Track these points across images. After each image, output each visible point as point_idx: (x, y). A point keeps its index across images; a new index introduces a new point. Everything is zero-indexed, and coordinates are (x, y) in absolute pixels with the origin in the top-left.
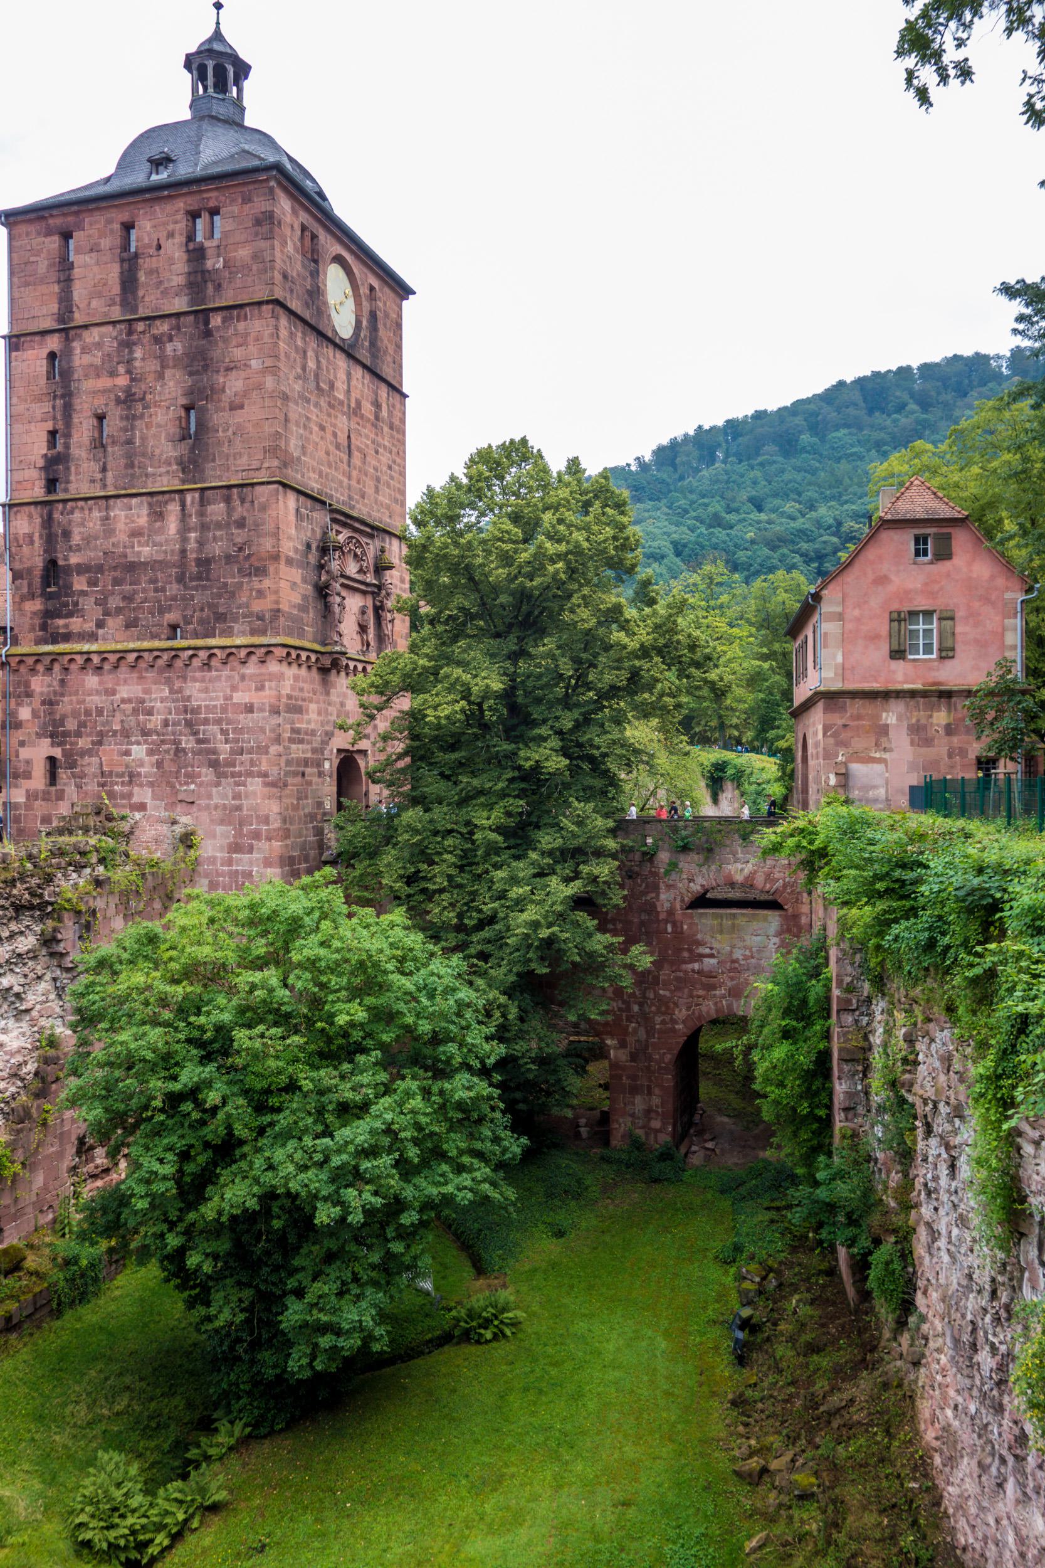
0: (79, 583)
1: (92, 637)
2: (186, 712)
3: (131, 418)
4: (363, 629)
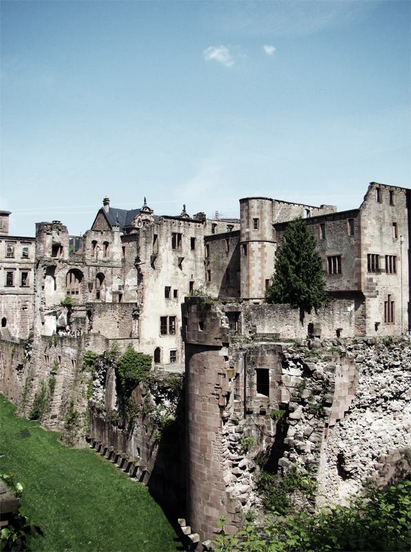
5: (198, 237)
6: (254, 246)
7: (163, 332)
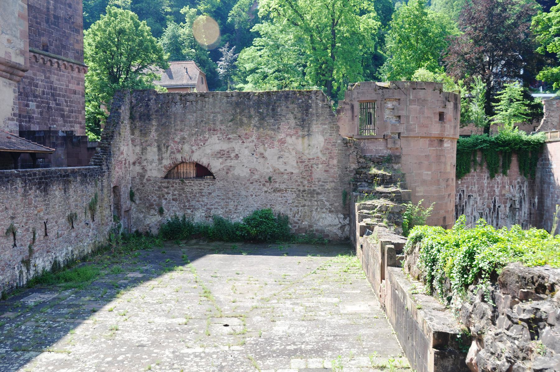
2: (51, 89)
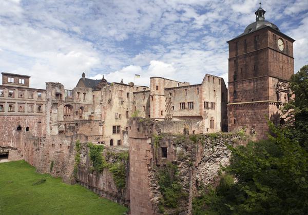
0: (239, 94)
1: (240, 102)
3: (246, 68)
4: (285, 98)
5: (130, 93)
6: (156, 97)
7: (114, 132)
